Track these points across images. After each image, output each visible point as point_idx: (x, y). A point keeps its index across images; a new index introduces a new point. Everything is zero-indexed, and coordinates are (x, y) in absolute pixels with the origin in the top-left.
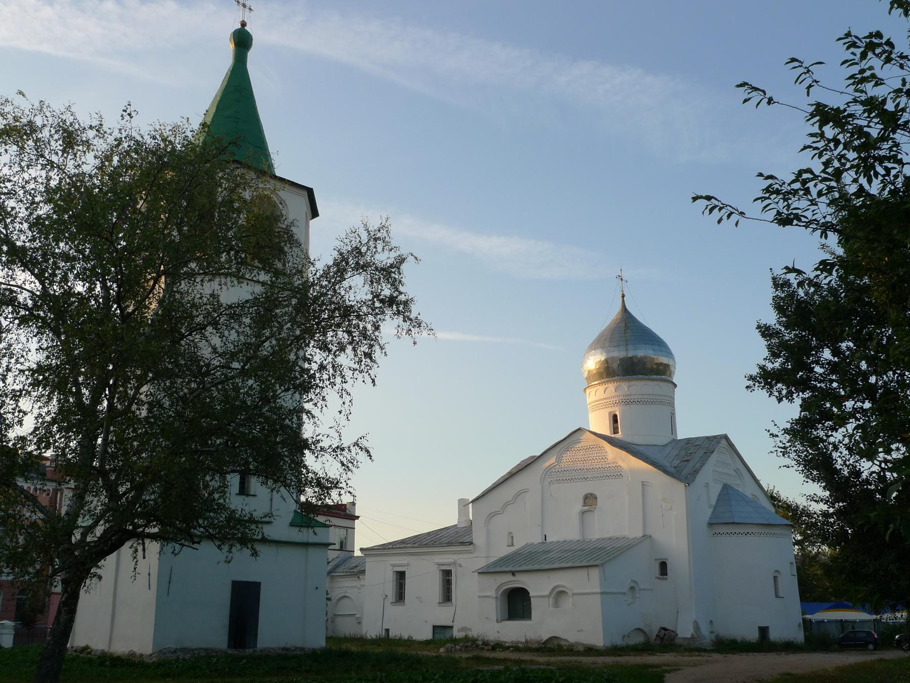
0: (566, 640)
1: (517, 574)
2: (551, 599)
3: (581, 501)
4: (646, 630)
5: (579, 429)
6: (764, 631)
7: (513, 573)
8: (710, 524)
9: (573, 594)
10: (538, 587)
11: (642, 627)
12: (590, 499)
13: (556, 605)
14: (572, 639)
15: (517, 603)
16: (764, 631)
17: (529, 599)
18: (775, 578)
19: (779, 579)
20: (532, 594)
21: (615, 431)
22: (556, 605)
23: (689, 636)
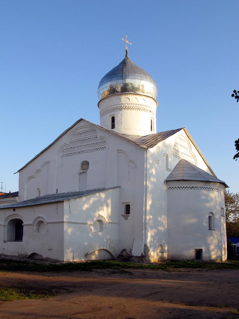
0: (41, 256)
1: (17, 210)
2: (35, 228)
3: (80, 166)
4: (111, 251)
5: (81, 120)
6: (199, 252)
7: (14, 209)
8: (167, 182)
9: (48, 223)
10: (28, 217)
11: (108, 249)
12: (85, 165)
13: (38, 230)
14: (45, 256)
15: (17, 229)
16: (199, 252)
17: (22, 227)
18: (210, 217)
19: (212, 218)
20: (25, 223)
21: (113, 126)
22: (38, 230)
23: (140, 255)
